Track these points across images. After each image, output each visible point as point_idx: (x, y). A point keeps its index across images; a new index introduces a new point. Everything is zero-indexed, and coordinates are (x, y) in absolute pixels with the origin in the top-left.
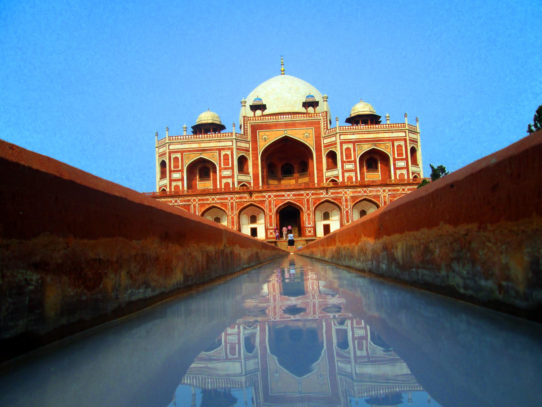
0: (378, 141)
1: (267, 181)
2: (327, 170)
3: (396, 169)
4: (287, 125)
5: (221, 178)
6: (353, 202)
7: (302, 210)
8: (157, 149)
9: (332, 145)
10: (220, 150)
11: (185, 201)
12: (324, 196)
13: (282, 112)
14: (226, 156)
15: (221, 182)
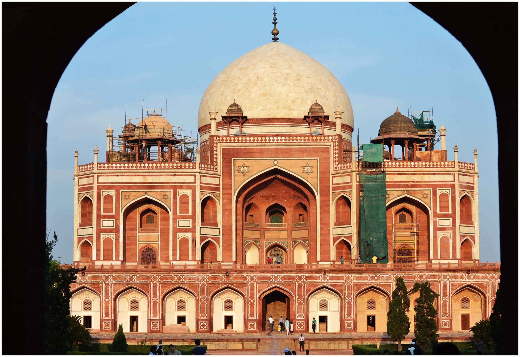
0: (412, 186)
1: (243, 234)
2: (336, 225)
3: (436, 229)
4: (278, 152)
5: (176, 230)
6: (356, 290)
7: (292, 297)
8: (76, 178)
9: (344, 188)
10: (175, 188)
11: (143, 279)
12: (321, 280)
13: (271, 117)
14: (184, 197)
15: (175, 237)
